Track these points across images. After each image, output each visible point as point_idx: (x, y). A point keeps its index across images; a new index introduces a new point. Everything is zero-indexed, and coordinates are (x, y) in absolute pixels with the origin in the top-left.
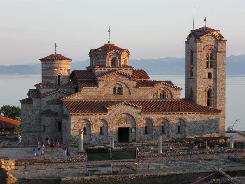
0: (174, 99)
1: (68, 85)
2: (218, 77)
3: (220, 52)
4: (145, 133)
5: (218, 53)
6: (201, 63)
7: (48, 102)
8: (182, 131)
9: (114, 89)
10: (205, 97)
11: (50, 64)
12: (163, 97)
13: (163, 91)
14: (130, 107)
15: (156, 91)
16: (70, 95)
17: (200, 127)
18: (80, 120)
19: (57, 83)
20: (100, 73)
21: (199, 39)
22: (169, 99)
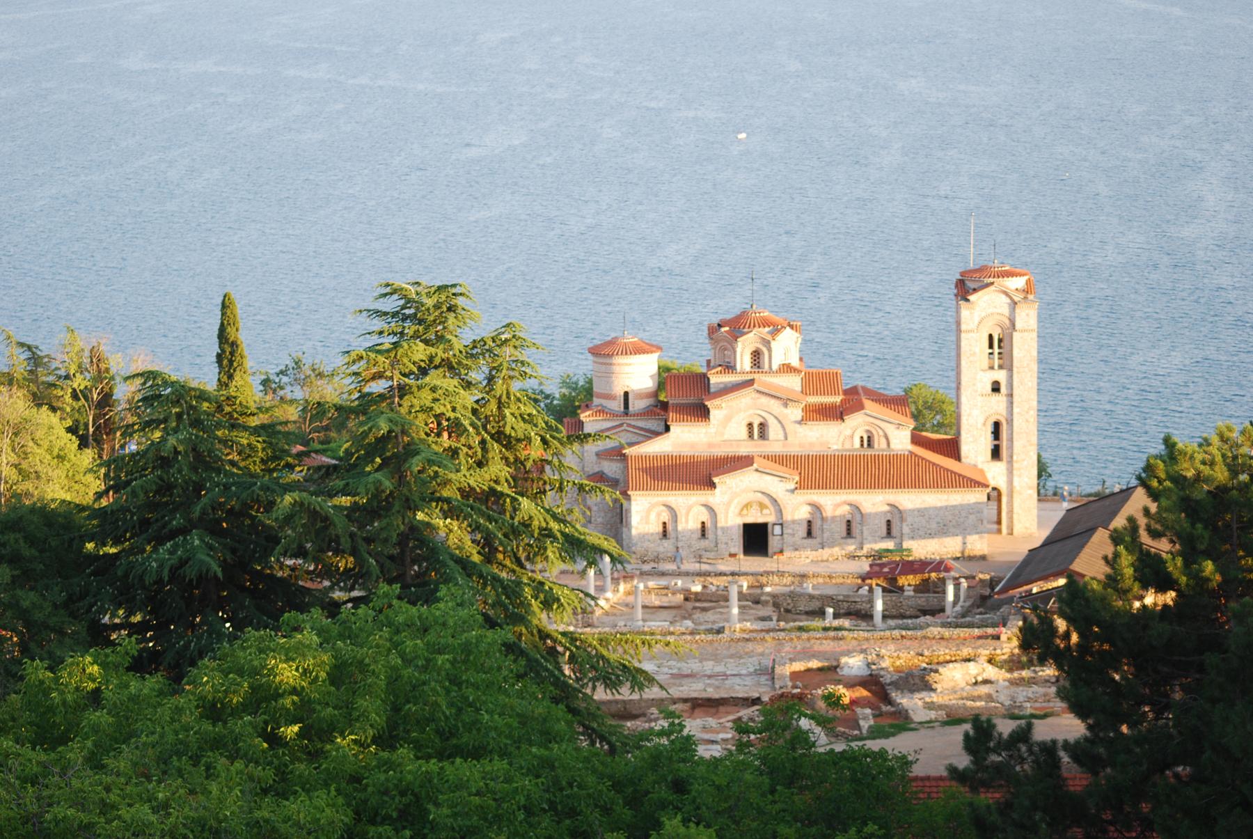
0: (893, 450)
1: (647, 413)
2: (1015, 392)
3: (1022, 331)
4: (805, 535)
5: (1015, 334)
6: (971, 359)
7: (598, 454)
8: (895, 531)
9: (750, 425)
10: (983, 439)
11: (605, 364)
12: (869, 445)
13: (868, 431)
14: (769, 478)
15: (848, 432)
16: (650, 438)
17: (938, 523)
18: (653, 506)
19: (622, 409)
20: (722, 386)
21: (968, 300)
22: (883, 450)
